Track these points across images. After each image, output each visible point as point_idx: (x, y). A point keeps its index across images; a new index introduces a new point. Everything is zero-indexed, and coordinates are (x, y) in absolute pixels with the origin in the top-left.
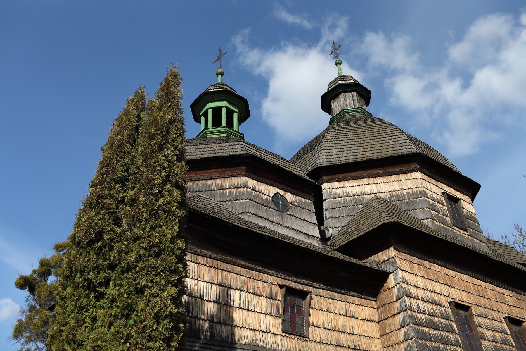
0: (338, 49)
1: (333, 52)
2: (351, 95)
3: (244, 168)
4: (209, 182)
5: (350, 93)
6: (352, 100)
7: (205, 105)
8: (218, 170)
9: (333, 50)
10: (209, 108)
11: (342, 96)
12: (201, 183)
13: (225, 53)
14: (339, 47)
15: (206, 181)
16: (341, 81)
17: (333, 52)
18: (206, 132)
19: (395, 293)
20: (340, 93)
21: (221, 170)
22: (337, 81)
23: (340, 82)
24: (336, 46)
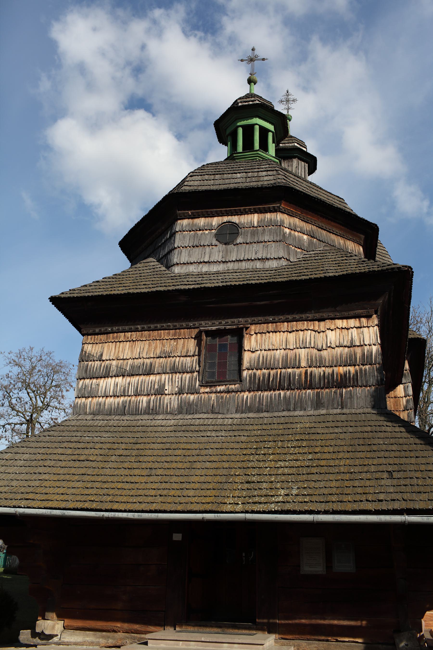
0: (292, 102)
1: (284, 102)
2: (303, 165)
3: (363, 237)
4: (333, 236)
5: (303, 163)
6: (304, 172)
7: (252, 117)
8: (341, 227)
9: (284, 100)
10: (257, 124)
11: (295, 161)
12: (324, 232)
13: (263, 59)
14: (294, 101)
15: (328, 233)
16: (298, 144)
17: (283, 101)
18: (258, 154)
19: (403, 403)
20: (295, 157)
21: (343, 228)
22: (294, 141)
23: (296, 144)
24: (289, 97)
